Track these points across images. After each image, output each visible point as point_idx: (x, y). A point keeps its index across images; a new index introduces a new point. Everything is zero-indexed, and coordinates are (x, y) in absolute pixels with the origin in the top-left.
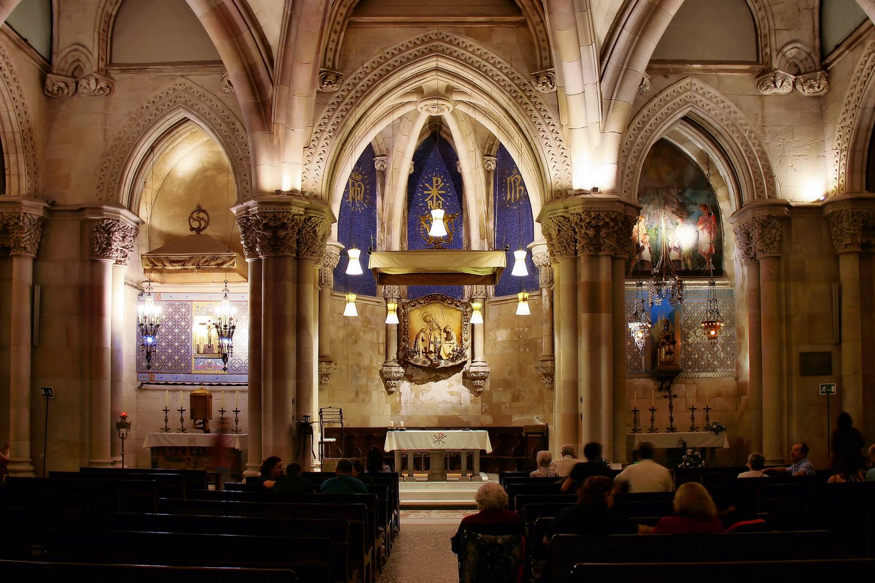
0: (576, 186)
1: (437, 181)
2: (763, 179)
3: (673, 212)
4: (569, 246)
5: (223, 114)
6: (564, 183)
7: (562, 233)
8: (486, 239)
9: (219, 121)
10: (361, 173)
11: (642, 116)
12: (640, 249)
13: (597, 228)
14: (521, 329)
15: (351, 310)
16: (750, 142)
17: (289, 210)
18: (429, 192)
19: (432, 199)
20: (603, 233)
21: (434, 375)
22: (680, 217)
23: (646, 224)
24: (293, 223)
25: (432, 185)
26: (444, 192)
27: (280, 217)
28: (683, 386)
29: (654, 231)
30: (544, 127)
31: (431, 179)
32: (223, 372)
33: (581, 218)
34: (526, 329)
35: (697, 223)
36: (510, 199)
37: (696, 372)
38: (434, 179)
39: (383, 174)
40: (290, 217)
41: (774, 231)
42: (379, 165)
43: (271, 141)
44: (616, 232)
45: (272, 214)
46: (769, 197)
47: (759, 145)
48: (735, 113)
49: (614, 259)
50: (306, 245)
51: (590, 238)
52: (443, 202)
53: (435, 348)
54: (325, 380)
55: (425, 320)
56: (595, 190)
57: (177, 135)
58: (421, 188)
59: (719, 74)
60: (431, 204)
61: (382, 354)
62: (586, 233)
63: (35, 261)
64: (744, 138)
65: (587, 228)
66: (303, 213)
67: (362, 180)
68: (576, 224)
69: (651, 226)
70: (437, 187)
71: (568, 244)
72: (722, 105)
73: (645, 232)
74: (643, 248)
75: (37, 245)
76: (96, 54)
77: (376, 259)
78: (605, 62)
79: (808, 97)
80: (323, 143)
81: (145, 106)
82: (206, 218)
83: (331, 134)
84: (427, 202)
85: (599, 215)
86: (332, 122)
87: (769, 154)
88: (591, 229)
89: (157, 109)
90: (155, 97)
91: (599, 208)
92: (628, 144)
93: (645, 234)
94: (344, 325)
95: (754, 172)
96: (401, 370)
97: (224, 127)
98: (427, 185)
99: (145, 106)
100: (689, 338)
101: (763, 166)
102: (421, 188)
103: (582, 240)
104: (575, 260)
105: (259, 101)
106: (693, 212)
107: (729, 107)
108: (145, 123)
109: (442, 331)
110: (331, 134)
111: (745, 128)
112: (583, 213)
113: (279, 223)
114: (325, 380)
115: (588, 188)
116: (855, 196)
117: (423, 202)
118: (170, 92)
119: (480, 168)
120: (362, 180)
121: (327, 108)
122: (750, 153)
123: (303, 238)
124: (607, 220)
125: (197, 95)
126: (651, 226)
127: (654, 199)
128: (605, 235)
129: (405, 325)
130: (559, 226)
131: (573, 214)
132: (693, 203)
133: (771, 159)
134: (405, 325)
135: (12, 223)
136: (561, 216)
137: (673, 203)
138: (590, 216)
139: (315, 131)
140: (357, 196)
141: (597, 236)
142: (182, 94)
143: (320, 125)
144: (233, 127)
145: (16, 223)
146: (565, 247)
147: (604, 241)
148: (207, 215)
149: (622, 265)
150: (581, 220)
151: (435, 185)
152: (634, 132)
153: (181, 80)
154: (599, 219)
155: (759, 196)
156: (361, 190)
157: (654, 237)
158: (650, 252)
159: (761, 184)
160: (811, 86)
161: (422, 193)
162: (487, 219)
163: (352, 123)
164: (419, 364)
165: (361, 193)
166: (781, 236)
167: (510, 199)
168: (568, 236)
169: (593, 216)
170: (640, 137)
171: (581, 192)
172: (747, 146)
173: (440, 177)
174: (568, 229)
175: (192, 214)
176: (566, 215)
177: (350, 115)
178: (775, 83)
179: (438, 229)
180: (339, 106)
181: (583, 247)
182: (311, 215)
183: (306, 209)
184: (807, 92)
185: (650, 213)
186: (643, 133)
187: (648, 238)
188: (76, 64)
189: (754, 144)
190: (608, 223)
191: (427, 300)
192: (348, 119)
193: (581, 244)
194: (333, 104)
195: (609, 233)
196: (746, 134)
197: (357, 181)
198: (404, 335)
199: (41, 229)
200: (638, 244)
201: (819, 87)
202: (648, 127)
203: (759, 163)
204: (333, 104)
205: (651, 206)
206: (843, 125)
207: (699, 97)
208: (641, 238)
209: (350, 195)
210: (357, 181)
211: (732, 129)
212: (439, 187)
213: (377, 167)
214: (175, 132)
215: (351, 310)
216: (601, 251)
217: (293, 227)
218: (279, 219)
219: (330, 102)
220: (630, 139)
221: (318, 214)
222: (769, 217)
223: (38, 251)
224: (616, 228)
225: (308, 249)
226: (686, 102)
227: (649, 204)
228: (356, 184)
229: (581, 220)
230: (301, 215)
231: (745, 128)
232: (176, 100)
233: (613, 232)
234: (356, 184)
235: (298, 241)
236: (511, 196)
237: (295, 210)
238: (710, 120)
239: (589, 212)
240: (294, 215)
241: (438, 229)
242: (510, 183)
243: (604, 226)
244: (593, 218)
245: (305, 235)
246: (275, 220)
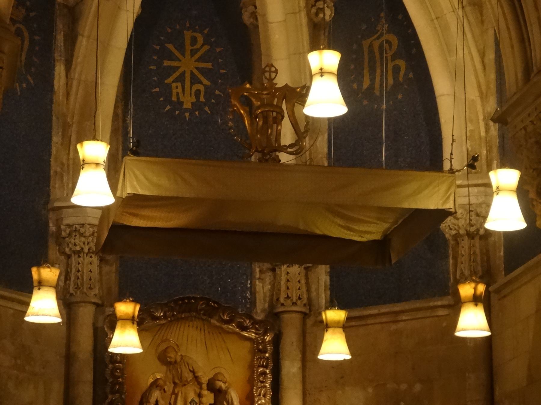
14: (404, 387)
18: (175, 64)
19: (181, 79)
25: (181, 48)
34: (418, 387)
36: (371, 87)
38: (188, 34)
60: (180, 90)
70: (193, 53)
77: (142, 178)
84: (169, 86)
98: (170, 46)
109: (205, 386)
134: (115, 369)
167: (371, 87)
173: (201, 32)
198: (113, 392)
212: (199, 54)
236: (373, 80)
242: (371, 51)
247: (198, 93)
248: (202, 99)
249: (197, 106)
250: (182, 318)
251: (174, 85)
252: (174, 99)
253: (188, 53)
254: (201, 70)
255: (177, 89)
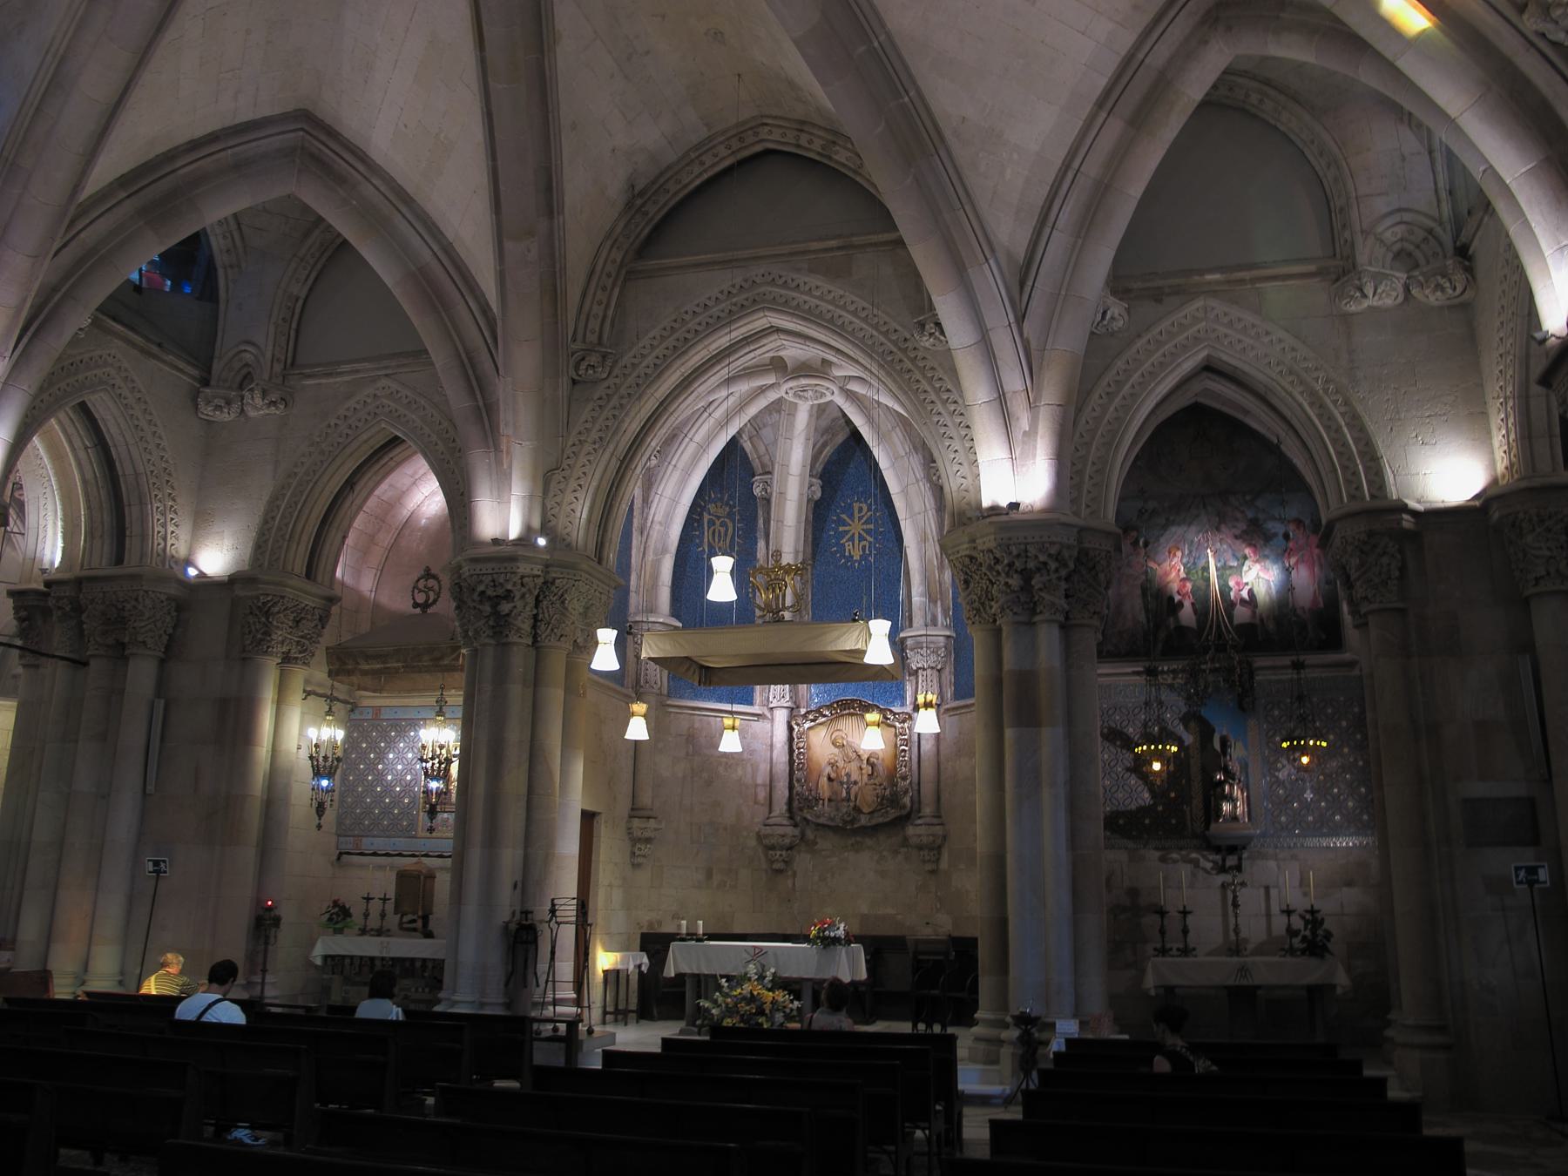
0: (986, 502)
1: (861, 510)
2: (1357, 465)
3: (1236, 537)
4: (984, 609)
5: (441, 427)
6: (971, 497)
7: (972, 585)
8: (939, 603)
9: (434, 438)
10: (727, 504)
11: (1114, 372)
12: (1174, 607)
13: (1026, 575)
15: (637, 730)
16: (1328, 401)
17: (514, 570)
18: (847, 528)
19: (852, 539)
20: (1037, 582)
21: (852, 841)
22: (1250, 545)
23: (1185, 560)
24: (524, 590)
25: (851, 516)
26: (872, 526)
27: (501, 581)
28: (1272, 864)
29: (1200, 572)
30: (939, 407)
31: (851, 506)
32: (428, 834)
33: (995, 558)
35: (1282, 555)
37: (1298, 836)
38: (856, 506)
39: (767, 501)
40: (516, 579)
41: (1385, 560)
42: (758, 490)
43: (499, 462)
44: (1067, 579)
45: (490, 578)
46: (1373, 496)
47: (1347, 403)
48: (1293, 349)
49: (1066, 628)
50: (549, 624)
51: (1015, 592)
52: (870, 543)
53: (848, 793)
54: (640, 849)
55: (834, 743)
56: (1014, 506)
57: (392, 464)
58: (834, 521)
59: (1258, 285)
61: (762, 805)
62: (1006, 583)
63: (162, 662)
64: (1312, 393)
65: (1007, 575)
66: (539, 573)
67: (730, 515)
68: (990, 568)
69: (1194, 563)
70: (860, 519)
71: (983, 604)
72: (1266, 340)
73: (1183, 575)
74: (1181, 604)
75: (165, 638)
76: (269, 355)
77: (653, 645)
78: (1030, 283)
79: (1441, 308)
80: (583, 459)
81: (332, 424)
82: (436, 588)
83: (596, 446)
84: (843, 545)
85: (1026, 551)
86: (597, 427)
87: (1366, 419)
88: (1015, 576)
89: (350, 427)
90: (348, 409)
91: (1025, 538)
92: (1091, 422)
93: (1183, 580)
94: (687, 754)
95: (1339, 454)
96: (790, 830)
97: (441, 447)
98: (844, 516)
99: (332, 424)
100: (1279, 771)
101: (1356, 441)
102: (834, 521)
103: (1000, 595)
104: (997, 633)
105: (481, 404)
106: (1275, 535)
107: (1280, 341)
108: (331, 449)
110: (596, 446)
111: (1315, 375)
112: (996, 548)
113: (500, 591)
114: (640, 849)
115: (1004, 503)
116: (1537, 482)
117: (837, 544)
118: (369, 401)
119: (921, 484)
120: (730, 515)
121: (590, 406)
122: (1329, 418)
123: (543, 613)
124: (1042, 558)
125: (405, 401)
126: (1194, 563)
127: (1197, 516)
128: (1040, 586)
129: (800, 753)
130: (966, 573)
131: (983, 552)
132: (1273, 518)
133: (1371, 427)
135: (128, 606)
136: (966, 556)
137: (1237, 520)
138: (1011, 553)
139: (570, 443)
140: (719, 541)
141: (1026, 587)
142: (385, 401)
143: (580, 433)
144: (453, 445)
145: (134, 607)
146: (978, 610)
147: (1040, 596)
148: (439, 582)
149: (1089, 640)
150: (997, 561)
151: (856, 515)
152: (1101, 402)
153: (384, 382)
154: (1027, 557)
155: (1352, 497)
156: (727, 531)
157: (1201, 583)
158: (1195, 611)
159: (1356, 473)
160: (1439, 287)
161: (836, 530)
162: (941, 568)
163: (633, 426)
164: (822, 821)
165: (726, 535)
166: (1403, 569)
168: (982, 588)
169: (1015, 552)
170: (1112, 409)
171: (995, 510)
172: (1321, 406)
173: (866, 502)
174: (981, 578)
175: (418, 581)
176: (975, 554)
177: (626, 415)
178: (1361, 290)
179: (722, 589)
180: (609, 401)
181: (1003, 609)
182: (554, 575)
183: (547, 566)
184: (1434, 298)
185: (1192, 542)
186: (1117, 401)
187: (1189, 585)
188: (244, 371)
189: (1335, 402)
190: (1045, 564)
191: (835, 709)
192: (623, 421)
193: (1000, 603)
194: (600, 398)
195: (1050, 580)
196: (1318, 387)
197: (719, 518)
199: (175, 614)
200: (1171, 599)
201: (1454, 289)
202: (1126, 389)
203: (1348, 436)
204: (600, 398)
205: (1193, 529)
206: (1502, 350)
207: (1222, 330)
208: (1175, 586)
209: (706, 540)
210: (719, 518)
211: (1291, 378)
213: (757, 491)
214: (386, 459)
215: (637, 730)
216: (1038, 614)
217: (523, 596)
218: (501, 585)
219: (596, 396)
220: (1095, 414)
221: (568, 574)
222: (1371, 534)
223: (168, 647)
224: (1064, 573)
225: (552, 630)
226: (1197, 340)
227: (1190, 524)
228: (718, 523)
229: (997, 561)
230: (539, 576)
231: (1315, 375)
232: (377, 411)
233: (1059, 579)
234: (718, 523)
235: (535, 617)
237: (524, 568)
238: (1246, 368)
239: (1008, 547)
240: (522, 577)
241: (722, 589)
243: (1039, 569)
244: (1018, 556)
245: (547, 608)
246: (495, 586)
247: (864, 548)
248: (867, 552)
249: (864, 557)
250: (843, 715)
251: (847, 544)
252: (847, 554)
253: (856, 520)
254: (868, 532)
255: (849, 546)
